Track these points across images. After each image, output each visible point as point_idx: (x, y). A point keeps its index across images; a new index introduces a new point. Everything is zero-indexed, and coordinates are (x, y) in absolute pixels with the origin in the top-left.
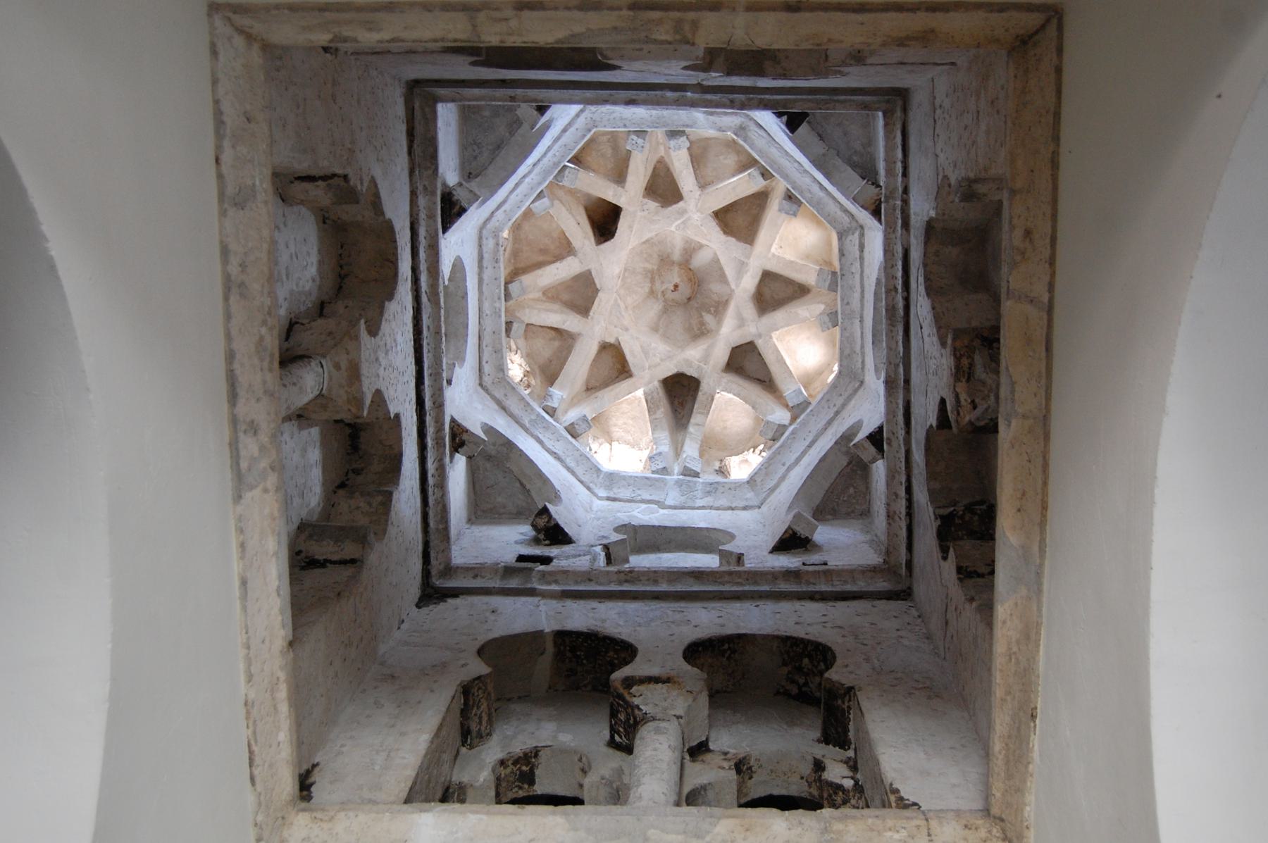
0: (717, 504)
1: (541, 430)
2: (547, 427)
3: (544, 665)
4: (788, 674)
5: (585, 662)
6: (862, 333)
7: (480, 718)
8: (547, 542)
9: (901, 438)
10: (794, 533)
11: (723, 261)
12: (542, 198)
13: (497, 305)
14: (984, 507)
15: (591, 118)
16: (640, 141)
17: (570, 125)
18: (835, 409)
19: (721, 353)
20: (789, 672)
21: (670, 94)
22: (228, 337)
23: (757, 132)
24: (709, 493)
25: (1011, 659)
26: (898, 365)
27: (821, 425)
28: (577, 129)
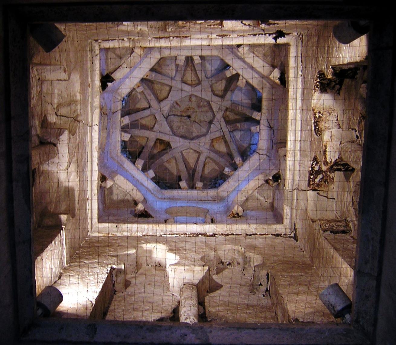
4: (331, 89)
7: (338, 226)
20: (330, 89)
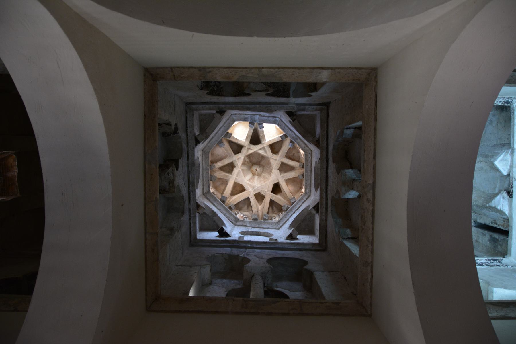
0: (244, 115)
2: (293, 138)
3: (292, 88)
5: (281, 88)
6: (203, 165)
8: (293, 112)
9: (190, 150)
12: (293, 202)
13: (306, 173)
14: (165, 136)
16: (265, 218)
18: (210, 143)
19: (244, 151)
21: (255, 246)
22: (373, 229)
24: (246, 118)
26: (191, 170)
27: (214, 139)
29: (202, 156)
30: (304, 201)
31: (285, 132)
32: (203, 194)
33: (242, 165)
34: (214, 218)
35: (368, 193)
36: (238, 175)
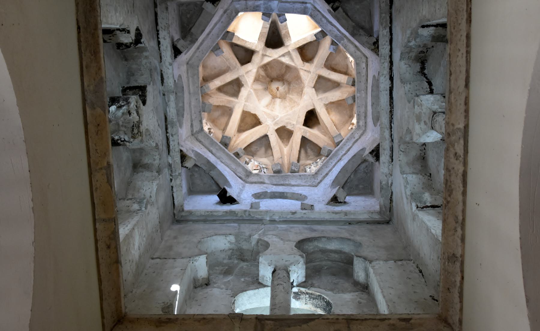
1: (338, 35)
2: (336, 36)
6: (189, 86)
10: (213, 4)
11: (257, 100)
12: (337, 142)
13: (359, 95)
15: (315, 179)
16: (293, 168)
17: (324, 177)
18: (199, 50)
19: (256, 59)
22: (464, 203)
23: (242, 175)
25: (94, 52)
28: (321, 174)
29: (188, 73)
30: (355, 139)
31: (323, 28)
32: (192, 135)
33: (254, 81)
34: (212, 172)
35: (456, 144)
36: (248, 99)
